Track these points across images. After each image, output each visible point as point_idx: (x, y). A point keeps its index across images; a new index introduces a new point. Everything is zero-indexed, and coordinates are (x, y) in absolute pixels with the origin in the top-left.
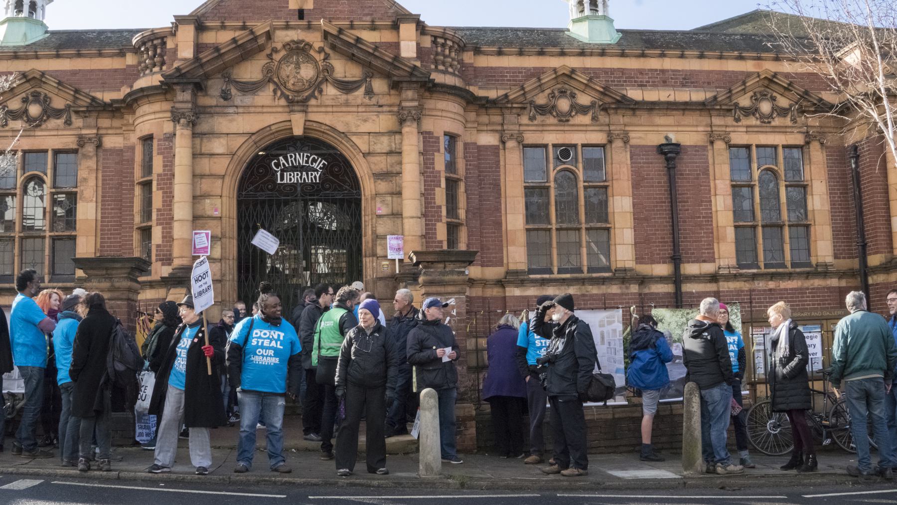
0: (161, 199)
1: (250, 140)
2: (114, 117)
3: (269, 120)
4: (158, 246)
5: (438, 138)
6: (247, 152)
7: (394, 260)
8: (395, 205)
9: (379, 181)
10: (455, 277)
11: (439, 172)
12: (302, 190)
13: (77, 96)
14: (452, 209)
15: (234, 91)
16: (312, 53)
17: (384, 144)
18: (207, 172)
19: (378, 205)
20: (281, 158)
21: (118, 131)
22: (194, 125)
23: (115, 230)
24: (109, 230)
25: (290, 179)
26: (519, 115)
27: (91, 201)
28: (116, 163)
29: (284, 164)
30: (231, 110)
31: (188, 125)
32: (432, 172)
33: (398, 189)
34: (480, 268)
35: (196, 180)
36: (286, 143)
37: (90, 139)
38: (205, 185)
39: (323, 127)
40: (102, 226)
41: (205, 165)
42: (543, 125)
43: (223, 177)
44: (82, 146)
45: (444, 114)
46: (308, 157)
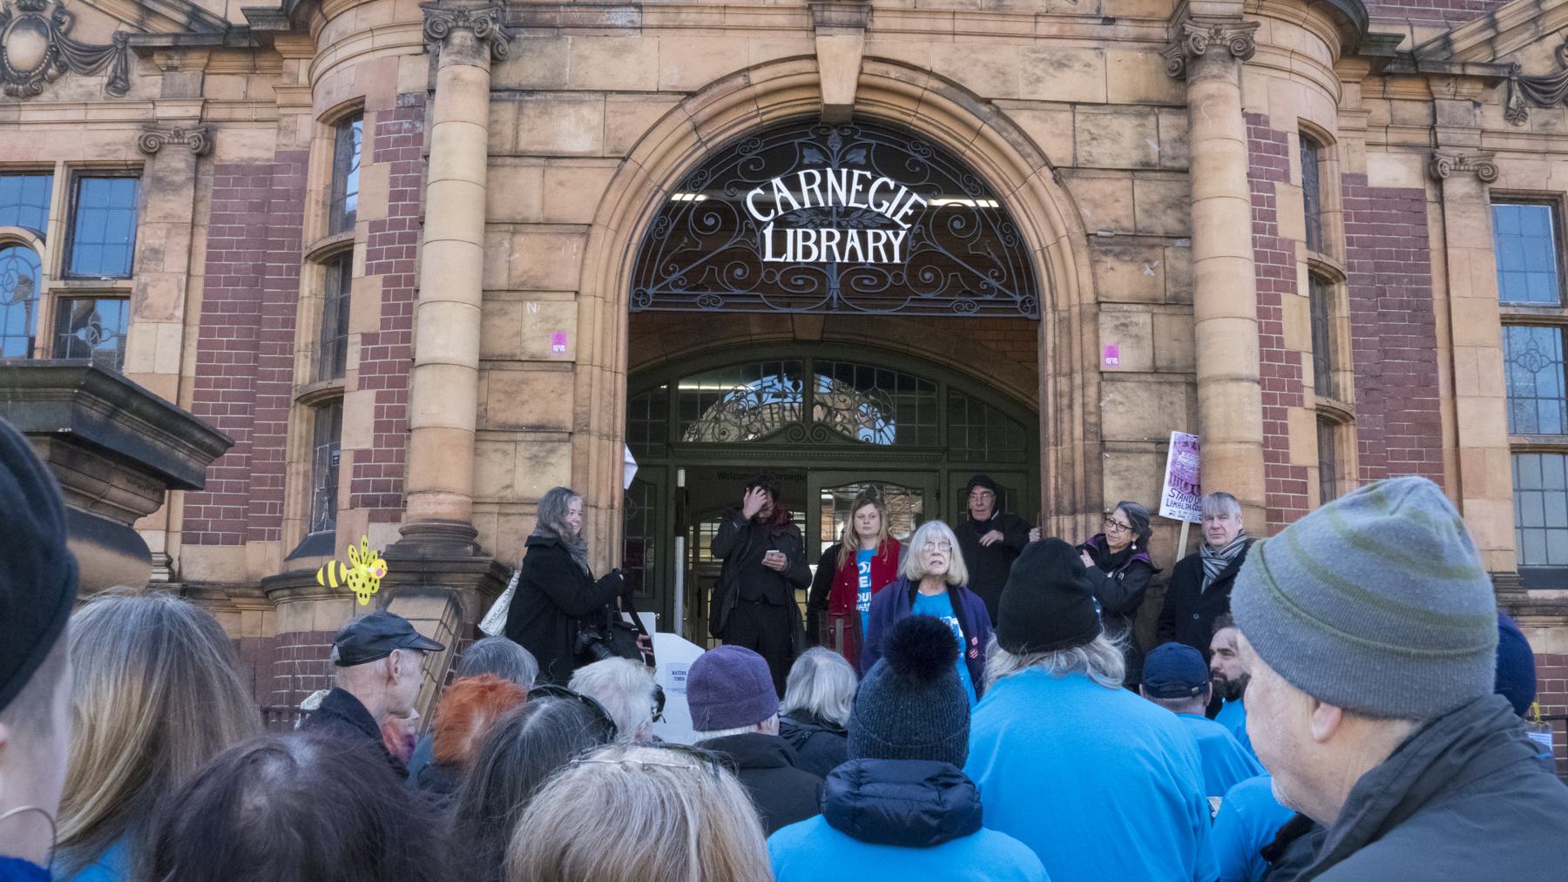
0: (377, 303)
1: (680, 115)
2: (254, 69)
3: (746, 50)
4: (360, 455)
5: (1283, 137)
6: (669, 153)
7: (1179, 523)
8: (1162, 342)
9: (1109, 261)
11: (1292, 243)
12: (844, 284)
17: (1122, 141)
18: (534, 213)
19: (1108, 338)
20: (777, 182)
21: (264, 113)
22: (496, 61)
23: (235, 410)
25: (807, 252)
26: (1477, 105)
27: (170, 318)
28: (254, 208)
29: (786, 204)
31: (477, 53)
32: (1272, 244)
33: (1171, 289)
35: (495, 238)
36: (794, 138)
37: (178, 133)
38: (524, 256)
39: (923, 80)
41: (528, 190)
42: (1548, 136)
44: (153, 154)
45: (1297, 65)
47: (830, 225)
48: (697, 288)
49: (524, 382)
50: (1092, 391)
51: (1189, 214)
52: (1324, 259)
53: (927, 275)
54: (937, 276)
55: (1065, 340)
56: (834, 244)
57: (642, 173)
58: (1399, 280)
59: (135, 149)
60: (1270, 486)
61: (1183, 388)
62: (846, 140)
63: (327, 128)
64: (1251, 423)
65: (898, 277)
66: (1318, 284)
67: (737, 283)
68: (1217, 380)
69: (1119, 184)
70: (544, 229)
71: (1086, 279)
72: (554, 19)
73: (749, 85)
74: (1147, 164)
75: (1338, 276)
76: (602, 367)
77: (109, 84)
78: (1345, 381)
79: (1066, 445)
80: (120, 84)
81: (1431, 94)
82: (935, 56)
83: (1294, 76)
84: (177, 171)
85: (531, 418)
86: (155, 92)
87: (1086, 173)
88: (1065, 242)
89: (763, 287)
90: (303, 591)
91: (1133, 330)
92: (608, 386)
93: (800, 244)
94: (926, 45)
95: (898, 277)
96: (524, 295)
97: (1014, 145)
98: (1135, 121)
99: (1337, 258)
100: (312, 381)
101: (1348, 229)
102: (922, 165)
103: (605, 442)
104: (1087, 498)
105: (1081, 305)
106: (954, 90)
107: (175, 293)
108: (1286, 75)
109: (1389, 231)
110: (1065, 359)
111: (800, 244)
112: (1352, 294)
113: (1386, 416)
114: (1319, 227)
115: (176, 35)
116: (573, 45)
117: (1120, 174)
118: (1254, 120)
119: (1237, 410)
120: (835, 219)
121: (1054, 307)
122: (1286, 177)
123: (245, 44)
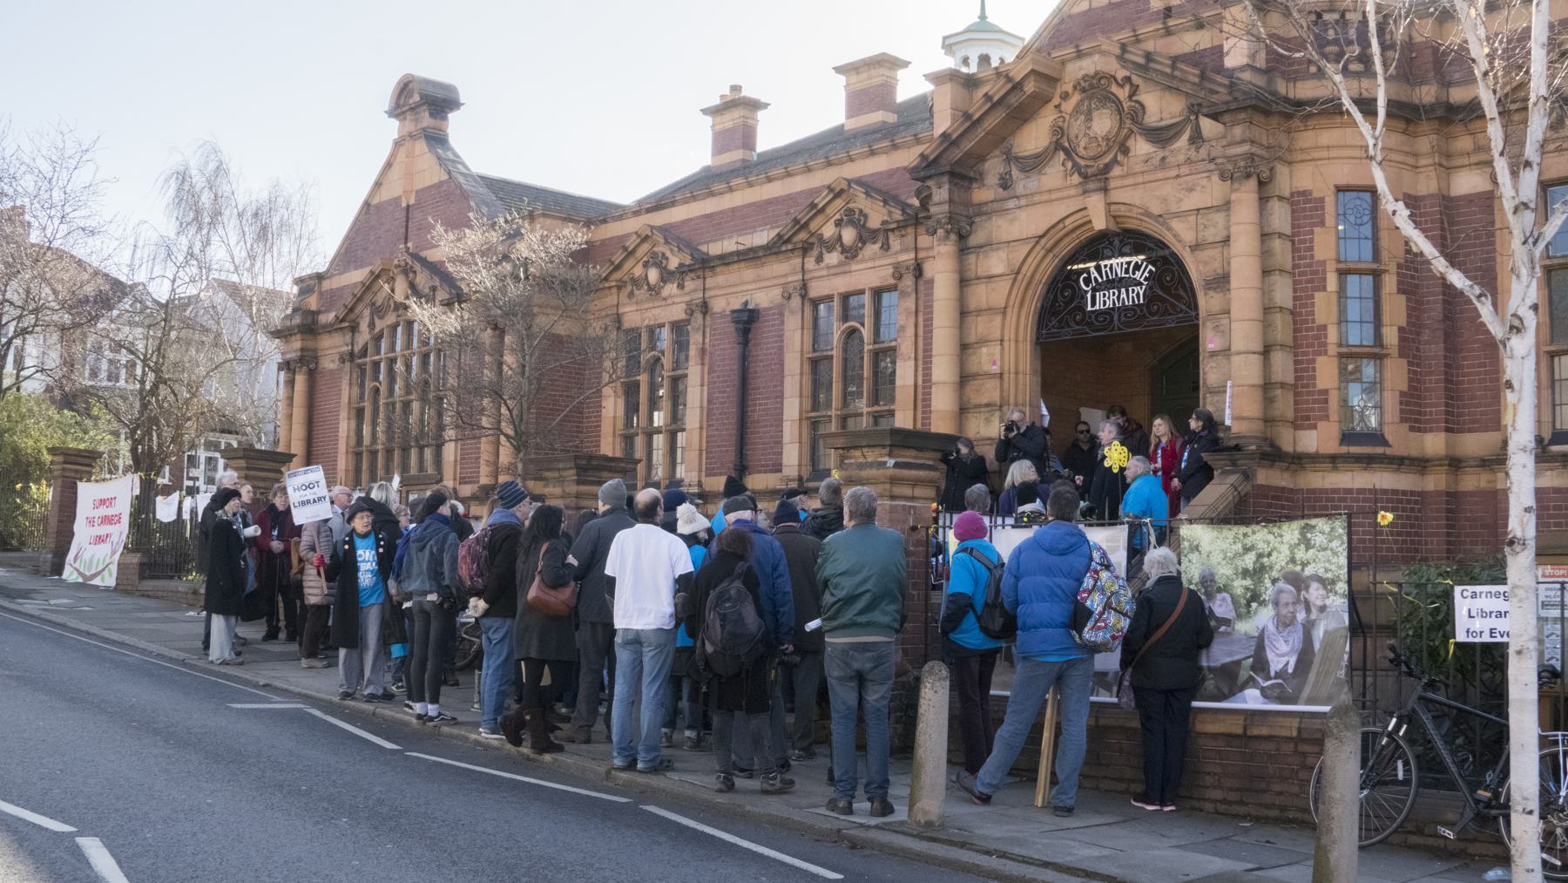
1: (1038, 247)
3: (1060, 210)
5: (1322, 200)
10: (874, 472)
15: (1015, 173)
16: (1114, 89)
18: (984, 305)
22: (962, 237)
30: (1011, 204)
32: (1310, 265)
34: (1443, 435)
43: (1004, 311)
45: (1334, 153)
85: (985, 401)
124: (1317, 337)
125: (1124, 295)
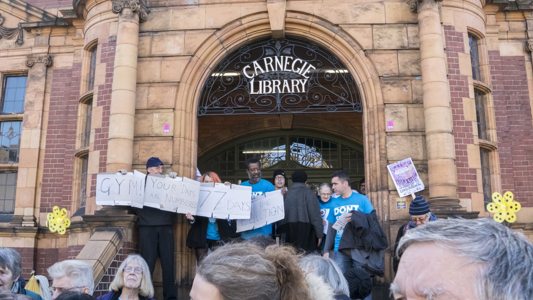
1: (214, 38)
2: (68, 34)
5: (461, 34)
8: (412, 118)
9: (388, 87)
11: (466, 77)
12: (283, 103)
13: (29, 11)
14: (482, 128)
17: (393, 38)
18: (157, 78)
19: (389, 118)
20: (255, 62)
21: (71, 49)
22: (142, 21)
24: (53, 161)
25: (267, 89)
27: (36, 127)
31: (133, 17)
32: (458, 78)
33: (415, 97)
37: (40, 59)
38: (153, 96)
39: (311, 18)
40: (46, 156)
41: (154, 70)
43: (177, 84)
44: (31, 67)
46: (290, 61)
47: (276, 78)
48: (224, 106)
49: (153, 145)
50: (383, 140)
51: (420, 66)
52: (481, 83)
53: (316, 97)
54: (320, 98)
55: (372, 120)
56: (278, 86)
57: (200, 62)
58: (515, 93)
59: (25, 65)
60: (459, 177)
61: (421, 137)
62: (283, 45)
63: (88, 52)
64: (449, 151)
65: (304, 98)
66: (479, 94)
67: (240, 104)
68: (433, 133)
69: (391, 56)
70: (161, 84)
71: (379, 94)
72: (165, 3)
73: (242, 25)
74: (403, 47)
75: (488, 90)
76: (185, 138)
77: (16, 42)
78: (493, 134)
79: (374, 163)
80: (20, 42)
81: (525, 18)
82: (315, 9)
83: (469, 15)
84: (39, 73)
86: (32, 44)
87: (378, 52)
88: (370, 80)
89: (250, 104)
90: (74, 229)
91: (399, 114)
92: (187, 145)
93: (265, 86)
94: (312, 5)
95: (304, 98)
96: (153, 110)
97: (348, 42)
98: (397, 30)
99: (487, 82)
100: (81, 148)
101: (492, 72)
102: (313, 53)
103: (187, 168)
104: (382, 184)
105: (377, 105)
106: (324, 22)
107: (38, 117)
108: (461, 10)
109: (510, 73)
110: (372, 128)
111: (265, 86)
112: (495, 98)
113: (512, 148)
114: (479, 71)
115: (38, 22)
116: (172, 13)
117: (392, 52)
118: (448, 29)
119: (442, 147)
120: (278, 76)
121: (367, 107)
122: (463, 50)
123: (63, 24)
124: (466, 130)
125: (286, 84)
